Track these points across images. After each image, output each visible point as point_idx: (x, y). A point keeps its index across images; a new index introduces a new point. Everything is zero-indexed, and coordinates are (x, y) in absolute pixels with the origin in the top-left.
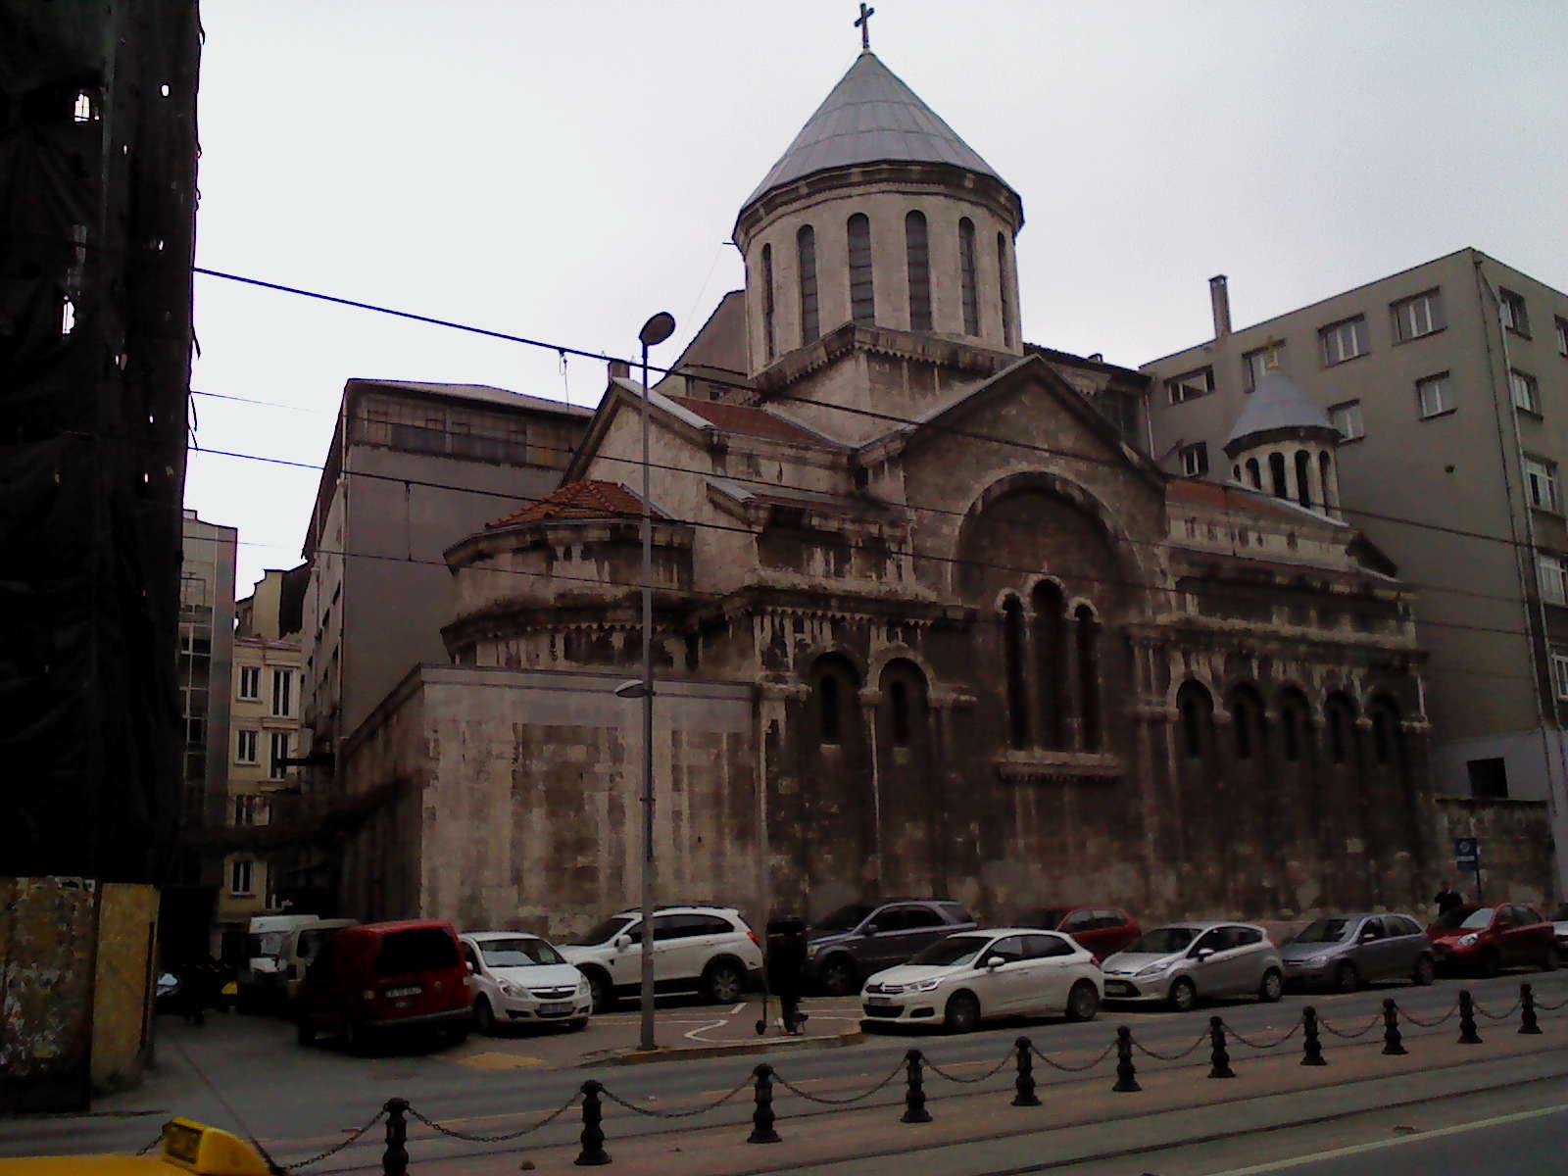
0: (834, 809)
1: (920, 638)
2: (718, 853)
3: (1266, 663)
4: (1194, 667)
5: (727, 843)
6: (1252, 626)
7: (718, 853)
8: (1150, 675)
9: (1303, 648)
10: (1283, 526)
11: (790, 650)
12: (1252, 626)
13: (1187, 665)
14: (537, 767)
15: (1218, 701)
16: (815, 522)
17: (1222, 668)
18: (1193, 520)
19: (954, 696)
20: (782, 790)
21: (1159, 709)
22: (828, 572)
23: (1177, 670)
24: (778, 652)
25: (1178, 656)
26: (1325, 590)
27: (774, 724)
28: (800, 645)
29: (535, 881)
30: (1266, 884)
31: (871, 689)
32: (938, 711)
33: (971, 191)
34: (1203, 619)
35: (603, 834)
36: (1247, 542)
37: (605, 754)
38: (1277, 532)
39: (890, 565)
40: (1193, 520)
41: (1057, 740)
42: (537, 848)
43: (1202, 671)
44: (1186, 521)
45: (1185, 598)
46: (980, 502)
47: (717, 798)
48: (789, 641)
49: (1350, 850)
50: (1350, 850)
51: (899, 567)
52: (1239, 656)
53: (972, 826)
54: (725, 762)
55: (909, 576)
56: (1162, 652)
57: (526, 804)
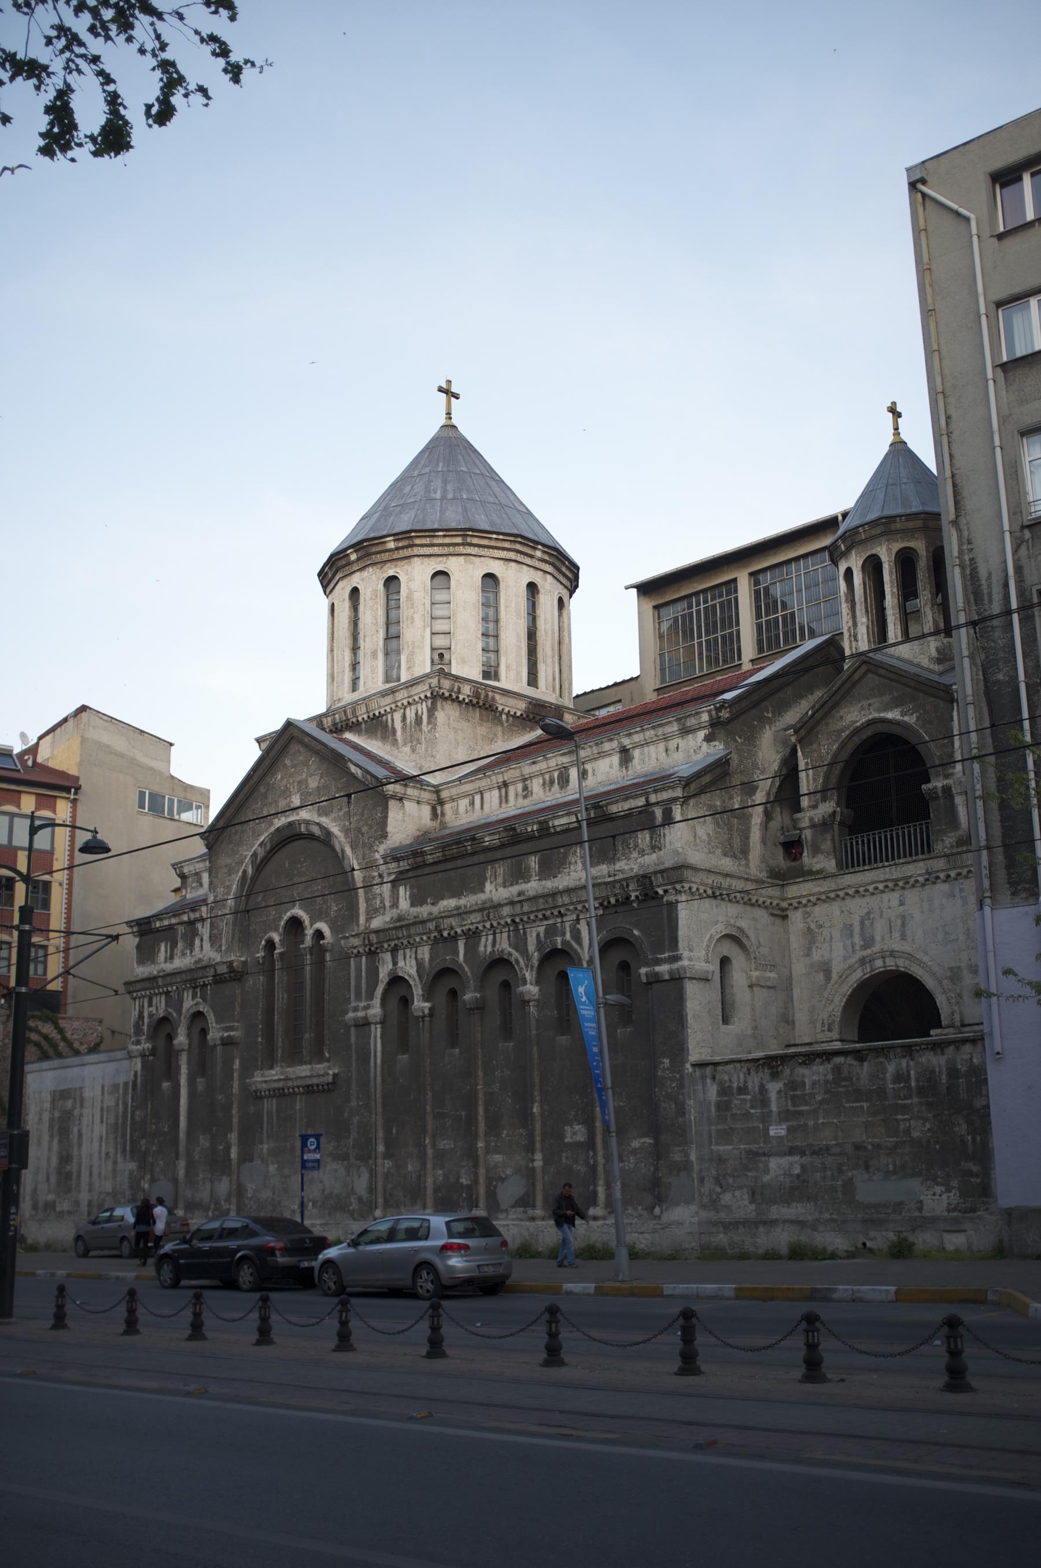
0: (166, 1129)
1: (209, 992)
2: (115, 1163)
3: (473, 936)
4: (401, 964)
5: (119, 1155)
6: (463, 901)
7: (115, 1163)
8: (361, 983)
9: (506, 911)
10: (607, 746)
11: (146, 1020)
12: (463, 901)
13: (395, 963)
14: (57, 1114)
15: (417, 991)
16: (158, 924)
17: (427, 957)
18: (505, 785)
19: (221, 1034)
20: (137, 1118)
21: (361, 1014)
22: (166, 958)
23: (384, 972)
24: (141, 1023)
25: (388, 957)
26: (545, 830)
27: (136, 1072)
28: (151, 1016)
29: (53, 1179)
30: (464, 1181)
31: (181, 1039)
32: (215, 1046)
33: (358, 559)
34: (415, 910)
35: (75, 1152)
36: (568, 781)
37: (78, 1105)
38: (602, 755)
39: (197, 941)
40: (505, 785)
41: (294, 1057)
42: (54, 1161)
43: (408, 967)
44: (499, 788)
45: (398, 894)
46: (250, 867)
47: (116, 1124)
48: (146, 1014)
49: (568, 1140)
50: (568, 1140)
51: (202, 940)
52: (444, 941)
53: (229, 1136)
54: (120, 1102)
55: (207, 945)
56: (372, 954)
57: (52, 1136)
